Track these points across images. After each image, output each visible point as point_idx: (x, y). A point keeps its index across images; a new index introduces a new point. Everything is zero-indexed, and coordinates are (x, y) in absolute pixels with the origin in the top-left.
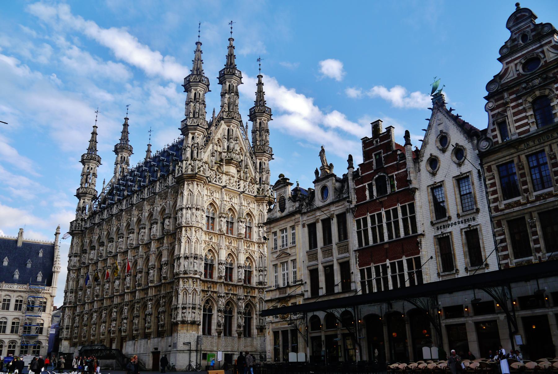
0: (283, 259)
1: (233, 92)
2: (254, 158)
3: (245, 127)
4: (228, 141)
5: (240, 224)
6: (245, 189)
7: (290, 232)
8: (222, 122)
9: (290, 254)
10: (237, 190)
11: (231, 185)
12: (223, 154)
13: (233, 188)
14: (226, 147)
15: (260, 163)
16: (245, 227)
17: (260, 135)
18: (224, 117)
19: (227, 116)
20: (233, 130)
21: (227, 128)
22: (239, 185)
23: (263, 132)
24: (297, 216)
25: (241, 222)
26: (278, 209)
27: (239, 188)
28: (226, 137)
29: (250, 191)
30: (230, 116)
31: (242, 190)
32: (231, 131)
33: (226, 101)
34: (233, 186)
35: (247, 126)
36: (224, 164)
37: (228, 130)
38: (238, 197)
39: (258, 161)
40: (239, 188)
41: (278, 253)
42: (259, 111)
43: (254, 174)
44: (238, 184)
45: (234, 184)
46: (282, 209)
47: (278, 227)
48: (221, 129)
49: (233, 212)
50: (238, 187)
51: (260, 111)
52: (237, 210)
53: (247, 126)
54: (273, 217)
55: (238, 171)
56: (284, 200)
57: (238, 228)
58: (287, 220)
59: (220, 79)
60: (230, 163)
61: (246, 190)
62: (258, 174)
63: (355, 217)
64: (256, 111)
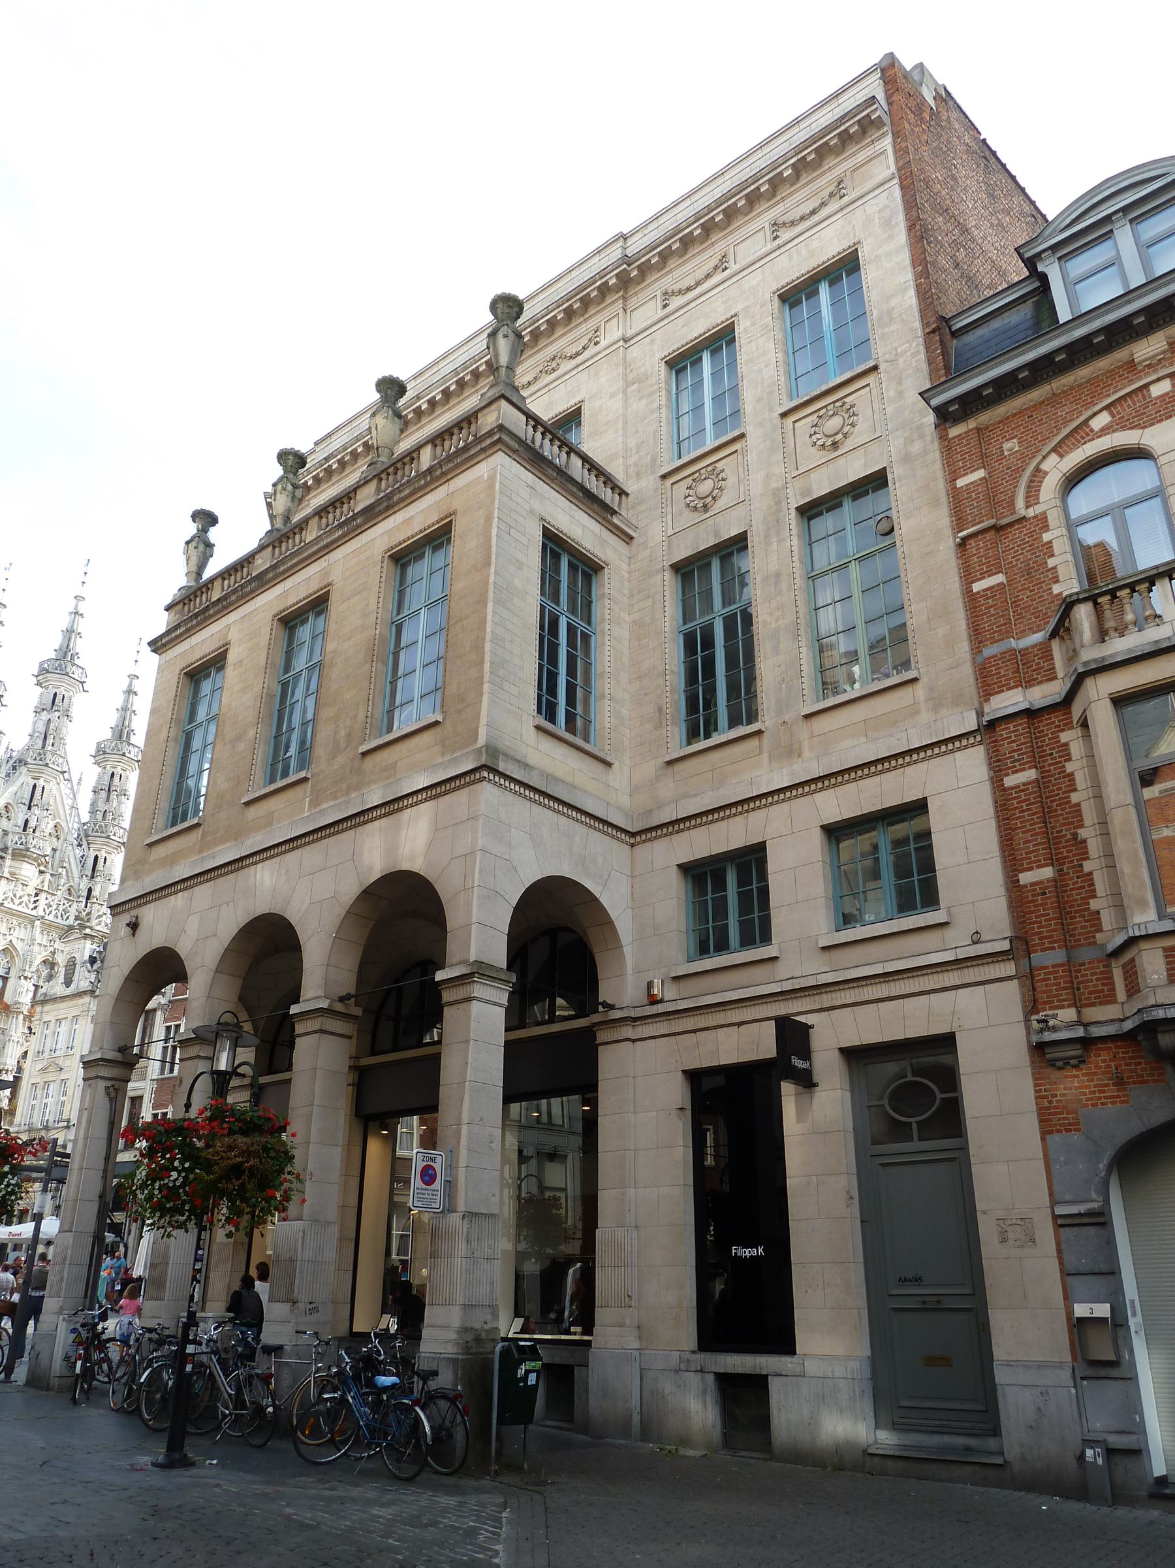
0: (50, 1075)
1: (59, 711)
2: (85, 846)
3: (75, 782)
4: (29, 808)
5: (23, 981)
6: (47, 911)
7: (64, 1029)
8: (24, 769)
9: (61, 1069)
10: (30, 912)
11: (17, 901)
12: (10, 836)
13: (20, 908)
14: (21, 823)
15: (96, 858)
16: (33, 988)
17: (108, 800)
18: (30, 761)
19: (35, 759)
20: (43, 788)
21: (32, 782)
22: (35, 902)
23: (113, 795)
24: (87, 999)
25: (26, 978)
26: (61, 979)
27: (35, 908)
28: (27, 803)
29: (59, 915)
30: (41, 760)
31: (42, 913)
32: (38, 791)
33: (41, 727)
34: (20, 903)
35: (80, 779)
36: (10, 857)
37: (35, 786)
38: (29, 927)
39: (92, 855)
40: (35, 908)
41: (45, 1062)
42: (113, 750)
43: (77, 880)
44: (33, 899)
45: (25, 899)
46: (68, 983)
47: (55, 1013)
48: (19, 783)
49: (12, 957)
50: (32, 906)
51: (115, 752)
52: (21, 953)
53: (80, 779)
54: (52, 992)
55: (41, 872)
56: (75, 965)
57: (16, 990)
58: (72, 1003)
59: (39, 678)
60: (25, 856)
61: (50, 912)
62: (85, 881)
63: (166, 1020)
64: (108, 751)
